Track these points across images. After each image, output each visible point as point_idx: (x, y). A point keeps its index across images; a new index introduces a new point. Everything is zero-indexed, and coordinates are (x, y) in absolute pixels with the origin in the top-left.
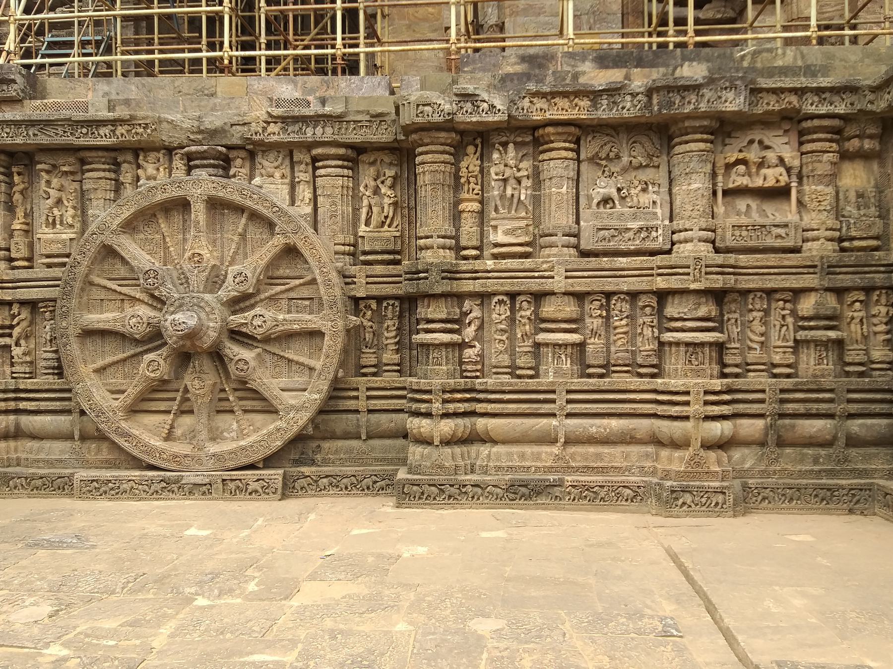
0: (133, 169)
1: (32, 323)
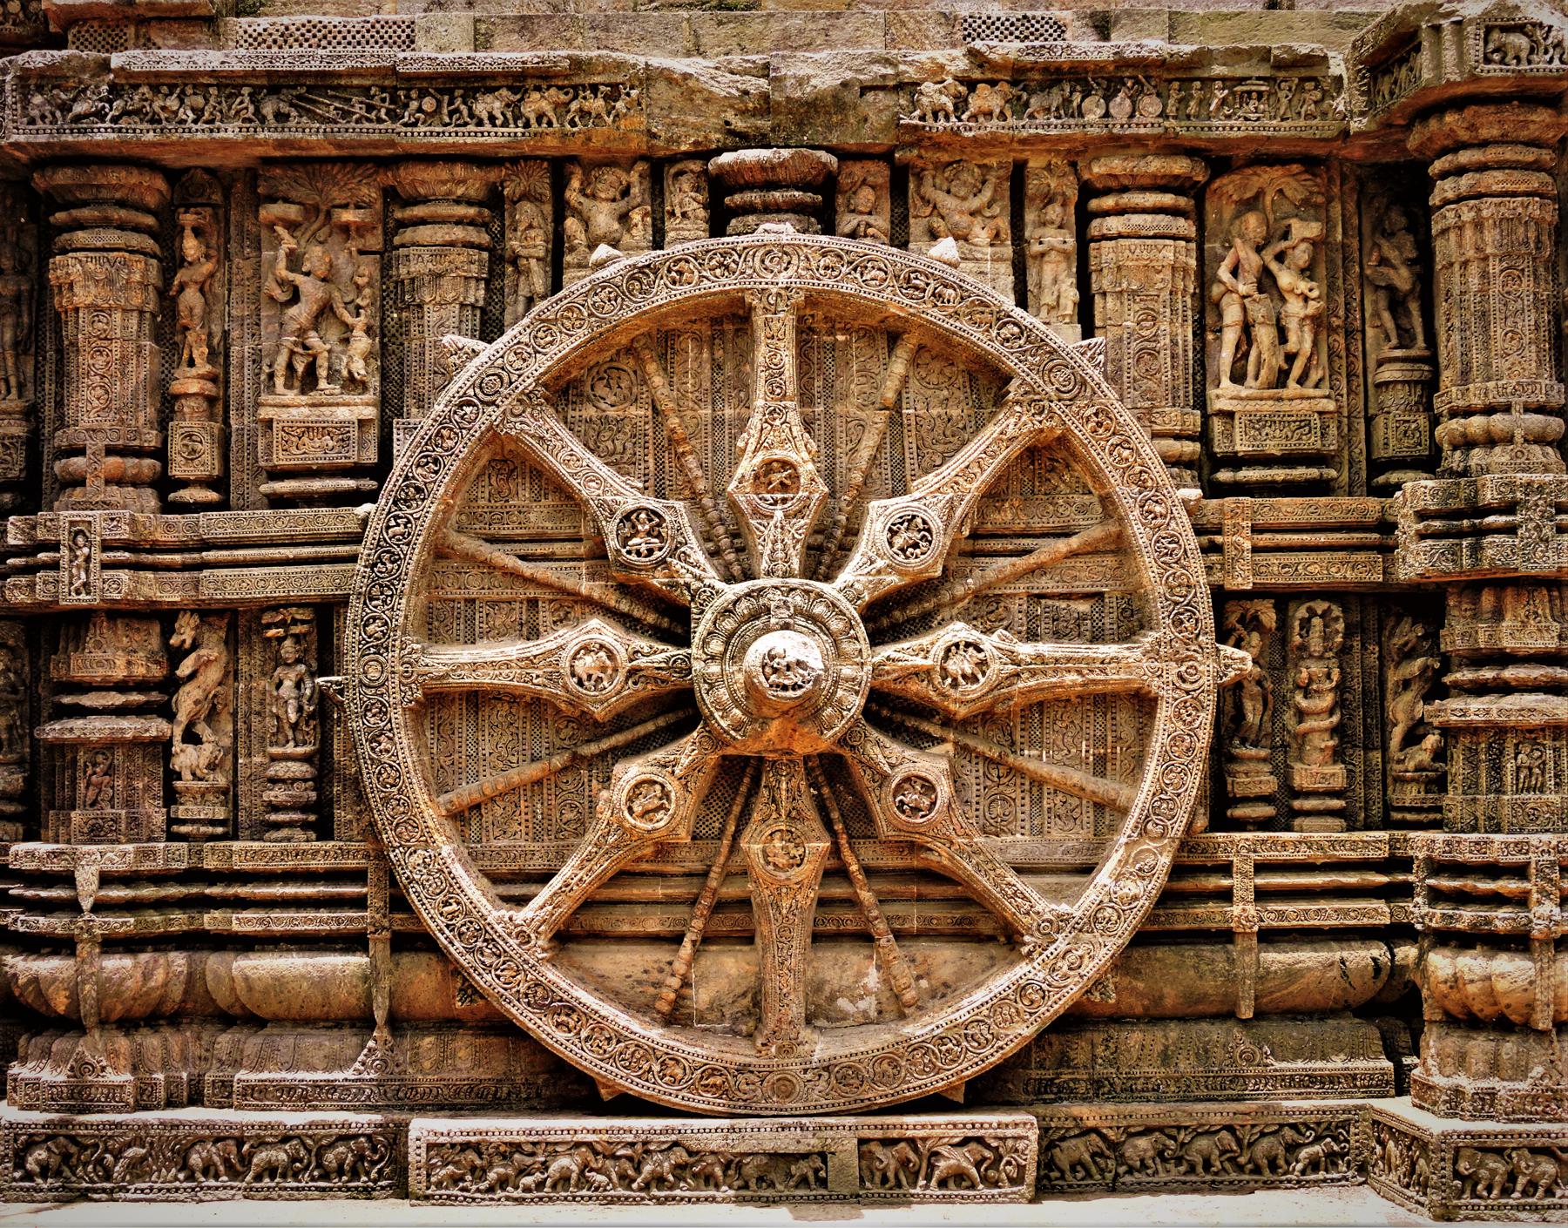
0: (545, 219)
1: (232, 673)
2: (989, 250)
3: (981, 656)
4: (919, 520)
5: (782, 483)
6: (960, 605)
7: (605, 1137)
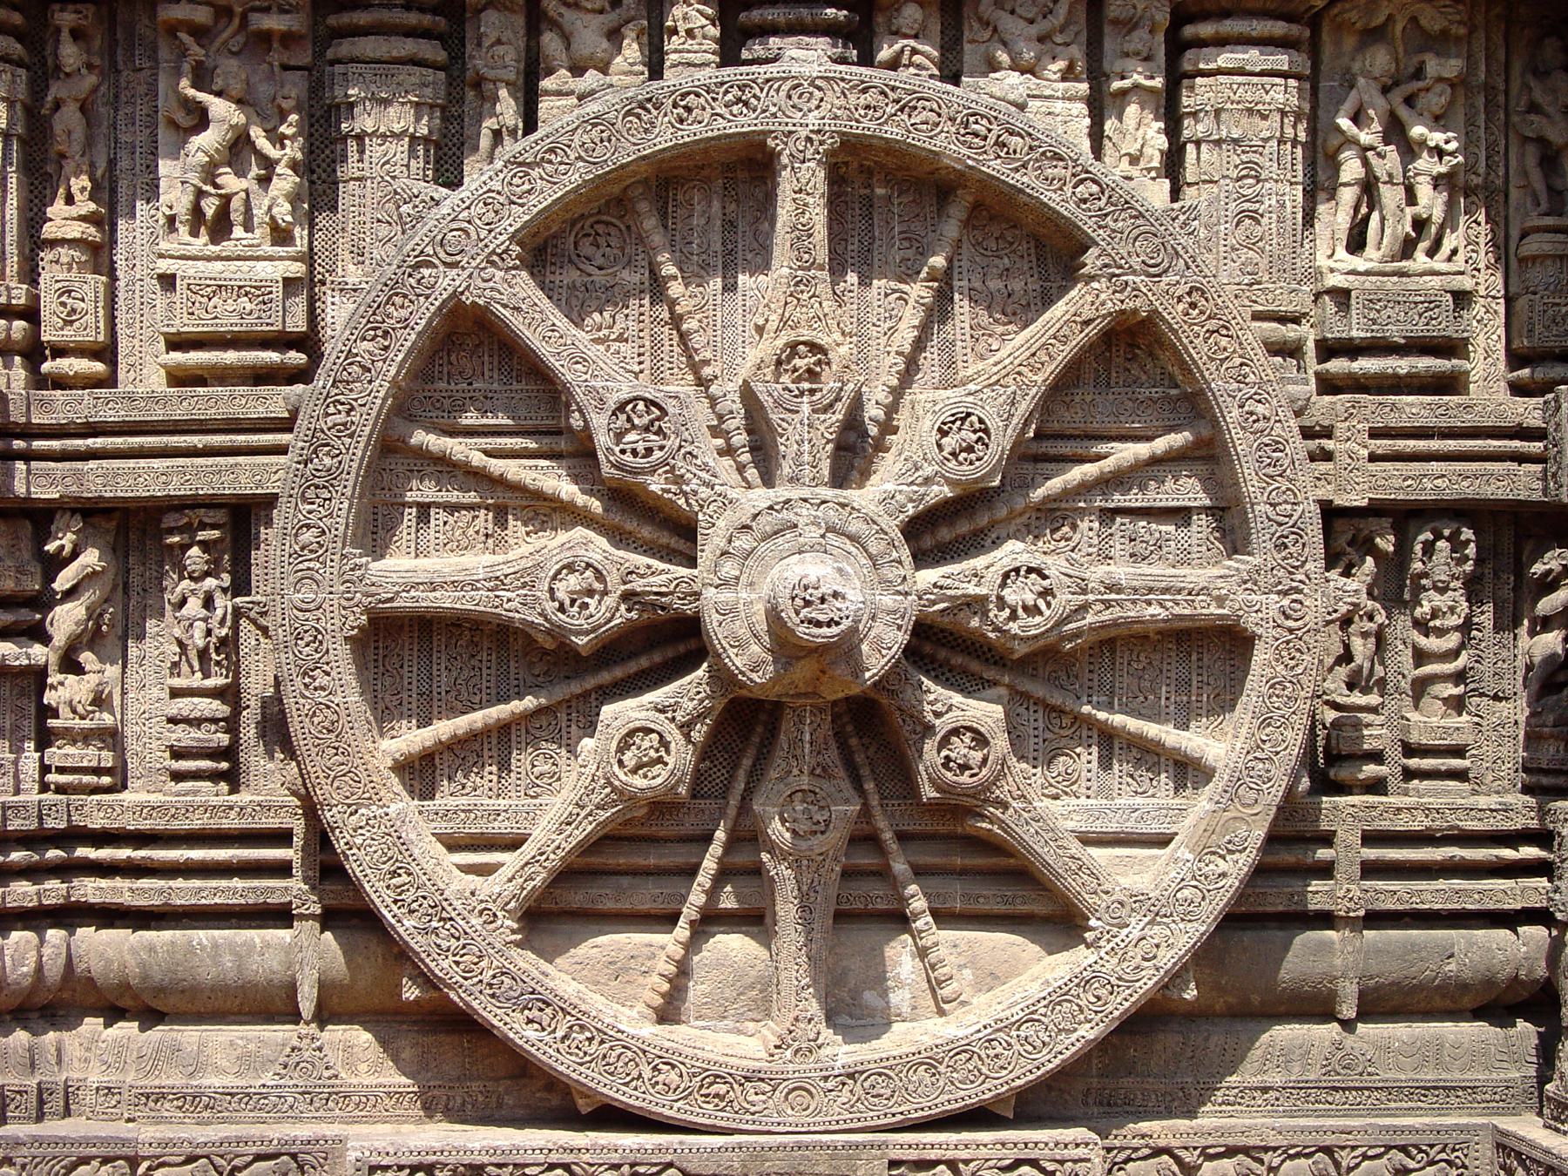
0: (515, 33)
2: (1062, 85)
3: (1046, 583)
4: (974, 418)
5: (809, 371)
6: (1018, 521)
7: (586, 1157)
